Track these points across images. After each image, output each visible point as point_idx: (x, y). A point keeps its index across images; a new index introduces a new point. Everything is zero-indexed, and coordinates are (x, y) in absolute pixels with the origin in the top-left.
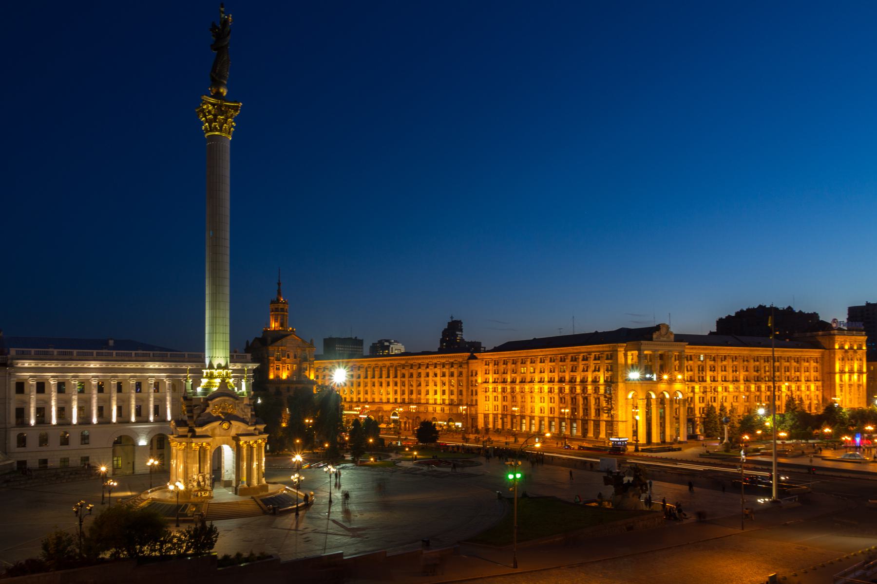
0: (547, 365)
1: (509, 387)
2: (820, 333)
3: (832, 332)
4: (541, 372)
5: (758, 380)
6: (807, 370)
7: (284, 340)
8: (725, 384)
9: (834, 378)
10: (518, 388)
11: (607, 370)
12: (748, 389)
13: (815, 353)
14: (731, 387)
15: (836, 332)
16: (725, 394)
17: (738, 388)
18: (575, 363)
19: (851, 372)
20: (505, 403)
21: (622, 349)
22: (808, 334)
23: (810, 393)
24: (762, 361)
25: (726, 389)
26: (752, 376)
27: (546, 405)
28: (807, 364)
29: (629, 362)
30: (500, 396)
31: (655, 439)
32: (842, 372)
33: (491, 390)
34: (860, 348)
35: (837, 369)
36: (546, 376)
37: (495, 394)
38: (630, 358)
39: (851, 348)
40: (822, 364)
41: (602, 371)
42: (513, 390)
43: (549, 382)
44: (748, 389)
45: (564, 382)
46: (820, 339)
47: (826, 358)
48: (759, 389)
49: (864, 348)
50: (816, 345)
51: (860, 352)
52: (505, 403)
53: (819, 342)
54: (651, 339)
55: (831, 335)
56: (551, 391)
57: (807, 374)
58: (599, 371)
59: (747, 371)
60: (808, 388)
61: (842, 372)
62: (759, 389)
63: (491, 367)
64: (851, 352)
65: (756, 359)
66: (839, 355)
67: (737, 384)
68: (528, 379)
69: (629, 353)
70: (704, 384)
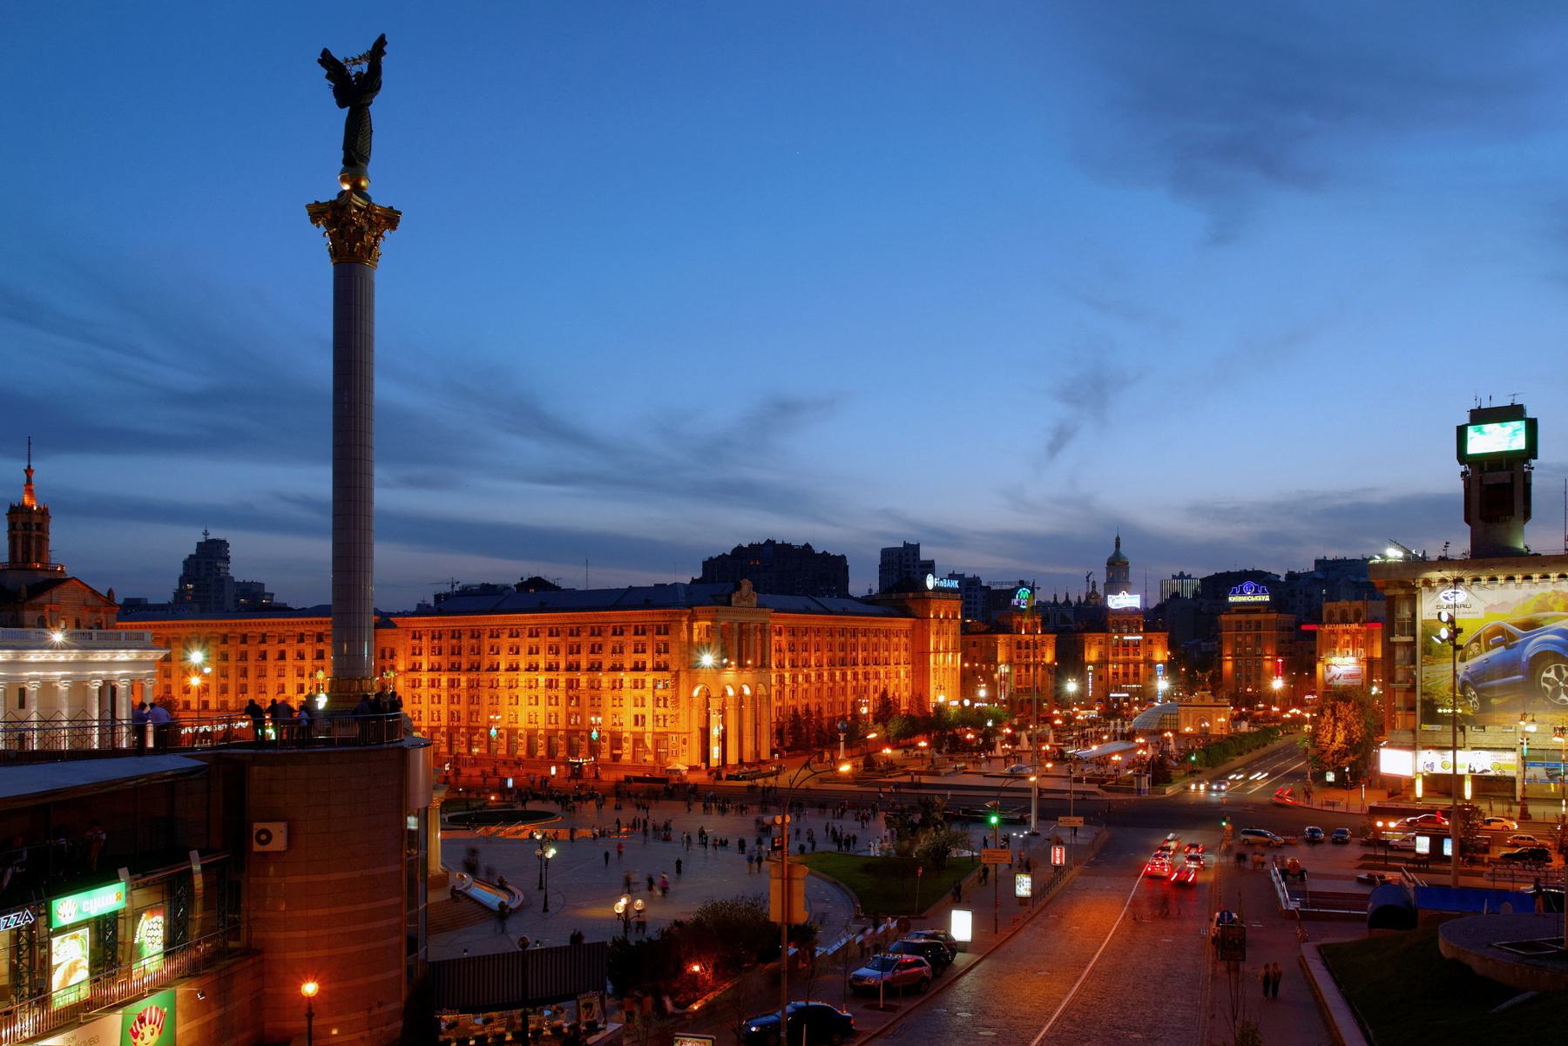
0: (543, 641)
1: (463, 678)
4: (530, 653)
5: (843, 663)
7: (55, 592)
10: (584, 679)
11: (659, 652)
12: (832, 676)
13: (904, 624)
18: (599, 639)
19: (946, 651)
20: (453, 707)
21: (685, 619)
22: (894, 596)
23: (898, 681)
27: (541, 710)
29: (696, 638)
30: (444, 695)
31: (732, 759)
33: (425, 684)
34: (955, 617)
36: (541, 660)
37: (434, 691)
38: (696, 632)
39: (946, 617)
40: (913, 640)
41: (649, 651)
42: (594, 686)
43: (589, 670)
44: (832, 676)
45: (578, 669)
48: (844, 676)
50: (905, 613)
52: (453, 707)
54: (729, 603)
56: (550, 684)
58: (644, 651)
60: (898, 673)
61: (937, 651)
62: (844, 676)
63: (425, 642)
64: (946, 622)
65: (843, 632)
66: (933, 627)
68: (486, 664)
69: (695, 625)
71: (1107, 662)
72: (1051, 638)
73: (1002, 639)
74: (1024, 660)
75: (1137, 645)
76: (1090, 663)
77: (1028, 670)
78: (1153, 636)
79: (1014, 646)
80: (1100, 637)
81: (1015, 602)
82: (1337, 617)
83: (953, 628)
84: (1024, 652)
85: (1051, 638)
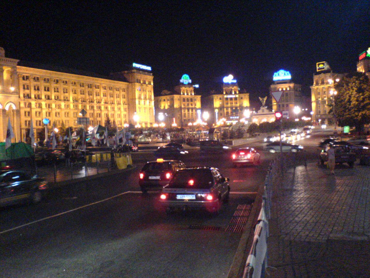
2: (126, 72)
3: (133, 71)
6: (118, 97)
8: (58, 102)
9: (135, 102)
13: (122, 85)
14: (63, 104)
15: (135, 71)
16: (58, 110)
17: (68, 106)
24: (87, 87)
25: (59, 107)
26: (79, 97)
28: (118, 92)
32: (140, 98)
34: (150, 84)
35: (137, 97)
40: (128, 94)
46: (125, 75)
47: (130, 89)
49: (152, 84)
51: (149, 86)
53: (125, 78)
55: (132, 72)
57: (118, 99)
59: (75, 93)
67: (67, 103)
70: (39, 101)
71: (224, 107)
72: (199, 97)
73: (176, 97)
74: (187, 107)
75: (236, 99)
76: (216, 108)
77: (188, 111)
78: (242, 95)
79: (182, 100)
80: (220, 96)
81: (181, 81)
82: (320, 82)
83: (150, 88)
84: (186, 103)
85: (199, 97)
